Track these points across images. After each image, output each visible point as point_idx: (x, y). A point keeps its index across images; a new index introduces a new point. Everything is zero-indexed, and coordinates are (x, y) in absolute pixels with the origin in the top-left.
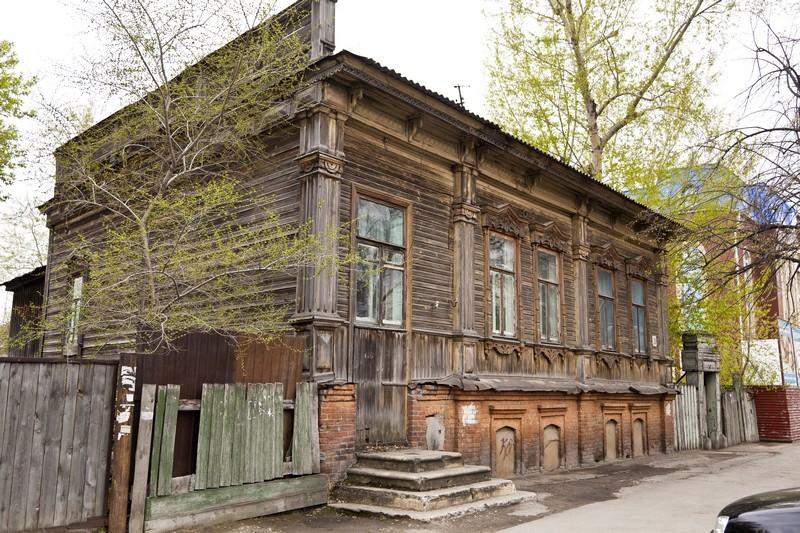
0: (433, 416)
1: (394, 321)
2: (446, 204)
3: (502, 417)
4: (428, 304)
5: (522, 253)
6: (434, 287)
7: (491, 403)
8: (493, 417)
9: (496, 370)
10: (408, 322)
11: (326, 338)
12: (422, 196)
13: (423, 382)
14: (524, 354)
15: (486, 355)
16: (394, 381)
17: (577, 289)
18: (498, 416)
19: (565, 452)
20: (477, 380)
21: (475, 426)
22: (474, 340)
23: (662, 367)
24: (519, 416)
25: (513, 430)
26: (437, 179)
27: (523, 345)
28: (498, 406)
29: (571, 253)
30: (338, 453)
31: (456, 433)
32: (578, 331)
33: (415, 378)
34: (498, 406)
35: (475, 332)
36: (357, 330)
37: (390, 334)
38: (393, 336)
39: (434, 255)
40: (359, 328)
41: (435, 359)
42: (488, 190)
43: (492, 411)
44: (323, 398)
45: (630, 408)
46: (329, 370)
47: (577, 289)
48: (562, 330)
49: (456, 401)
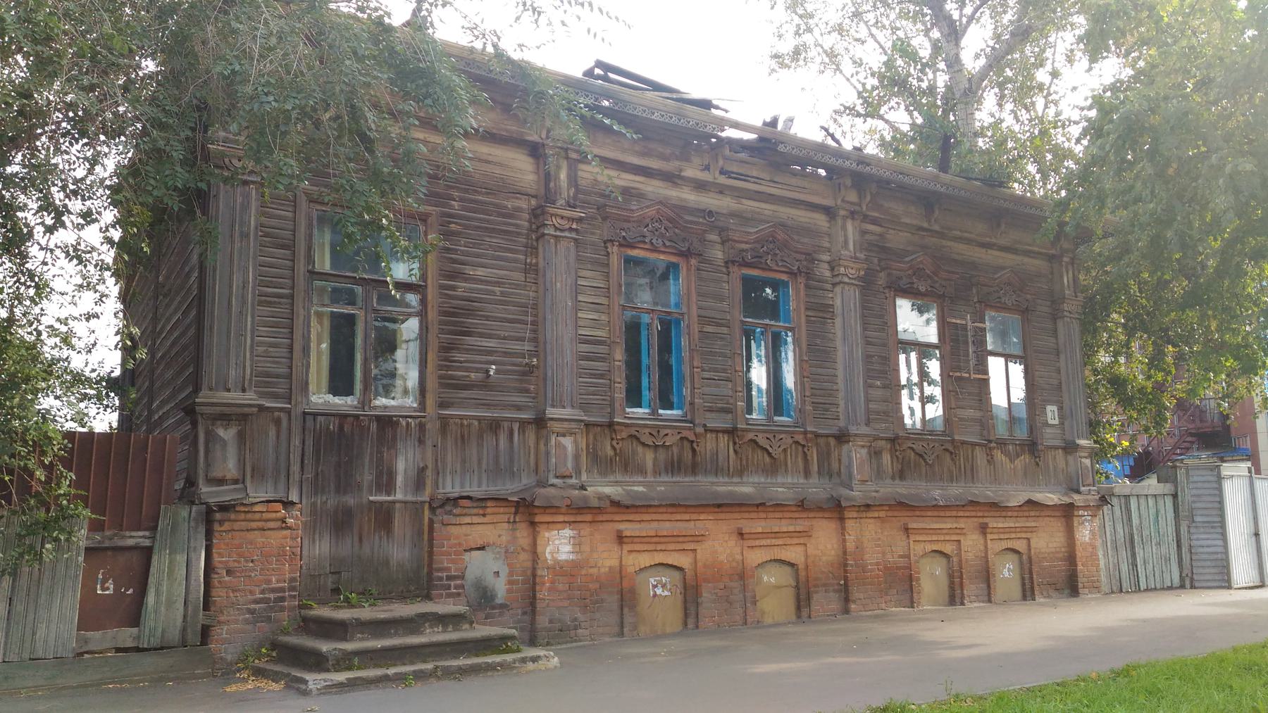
0: (482, 548)
1: (399, 400)
2: (519, 209)
3: (651, 547)
4: (477, 370)
5: (700, 279)
6: (491, 343)
7: (622, 526)
8: (626, 548)
9: (641, 470)
10: (430, 402)
11: (227, 434)
12: (461, 200)
13: (456, 495)
14: (702, 444)
15: (613, 447)
16: (399, 496)
17: (839, 334)
18: (638, 547)
19: (809, 598)
20: (583, 488)
21: (575, 565)
22: (573, 425)
23: (1070, 458)
24: (692, 546)
25: (680, 569)
26: (498, 171)
27: (700, 430)
28: (628, 529)
29: (828, 274)
30: (252, 612)
31: (534, 575)
32: (842, 403)
33: (449, 489)
34: (628, 529)
35: (576, 412)
36: (309, 419)
37: (387, 423)
38: (398, 423)
39: (493, 293)
40: (315, 415)
41: (497, 457)
42: (618, 182)
43: (621, 539)
44: (216, 527)
45: (983, 529)
46: (236, 482)
47: (839, 334)
48: (803, 402)
49: (533, 524)
